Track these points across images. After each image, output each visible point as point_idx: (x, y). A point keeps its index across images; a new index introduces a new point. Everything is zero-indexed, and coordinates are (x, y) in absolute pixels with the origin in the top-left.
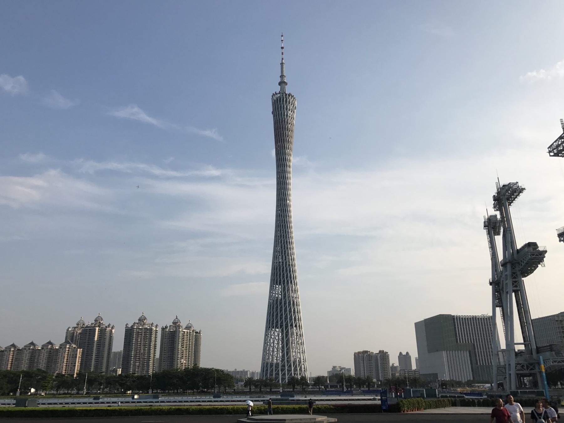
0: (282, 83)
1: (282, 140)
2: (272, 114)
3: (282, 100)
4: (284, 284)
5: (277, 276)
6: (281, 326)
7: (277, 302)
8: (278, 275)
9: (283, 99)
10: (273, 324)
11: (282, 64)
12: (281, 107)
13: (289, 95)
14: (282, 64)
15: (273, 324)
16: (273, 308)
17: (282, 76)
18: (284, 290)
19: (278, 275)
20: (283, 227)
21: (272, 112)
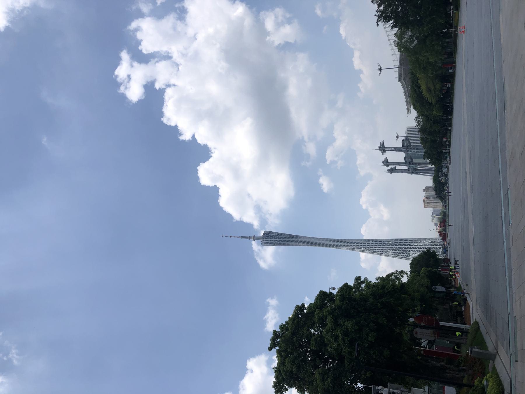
0: (255, 238)
1: (292, 242)
2: (273, 246)
3: (266, 240)
4: (384, 248)
5: (378, 251)
6: (410, 251)
7: (395, 253)
8: (374, 250)
9: (267, 239)
10: (408, 256)
11: (242, 237)
12: (271, 240)
13: (264, 235)
14: (242, 237)
15: (408, 256)
16: (399, 255)
17: (250, 238)
18: (388, 248)
19: (374, 250)
20: (348, 245)
21: (272, 246)
